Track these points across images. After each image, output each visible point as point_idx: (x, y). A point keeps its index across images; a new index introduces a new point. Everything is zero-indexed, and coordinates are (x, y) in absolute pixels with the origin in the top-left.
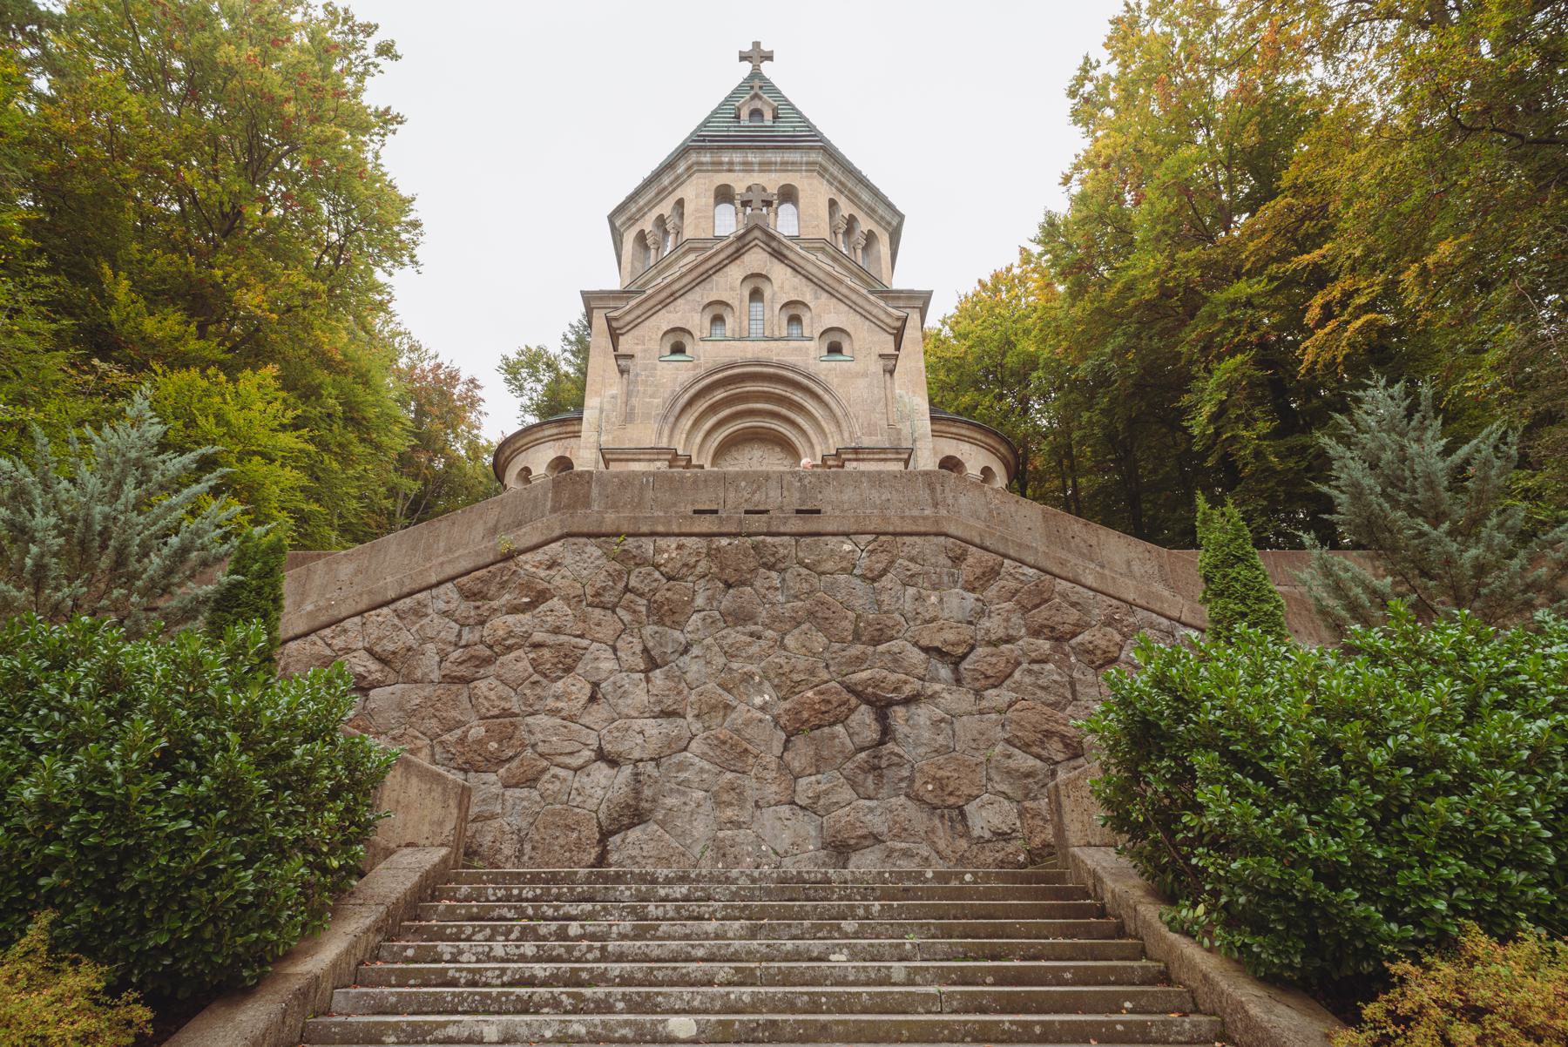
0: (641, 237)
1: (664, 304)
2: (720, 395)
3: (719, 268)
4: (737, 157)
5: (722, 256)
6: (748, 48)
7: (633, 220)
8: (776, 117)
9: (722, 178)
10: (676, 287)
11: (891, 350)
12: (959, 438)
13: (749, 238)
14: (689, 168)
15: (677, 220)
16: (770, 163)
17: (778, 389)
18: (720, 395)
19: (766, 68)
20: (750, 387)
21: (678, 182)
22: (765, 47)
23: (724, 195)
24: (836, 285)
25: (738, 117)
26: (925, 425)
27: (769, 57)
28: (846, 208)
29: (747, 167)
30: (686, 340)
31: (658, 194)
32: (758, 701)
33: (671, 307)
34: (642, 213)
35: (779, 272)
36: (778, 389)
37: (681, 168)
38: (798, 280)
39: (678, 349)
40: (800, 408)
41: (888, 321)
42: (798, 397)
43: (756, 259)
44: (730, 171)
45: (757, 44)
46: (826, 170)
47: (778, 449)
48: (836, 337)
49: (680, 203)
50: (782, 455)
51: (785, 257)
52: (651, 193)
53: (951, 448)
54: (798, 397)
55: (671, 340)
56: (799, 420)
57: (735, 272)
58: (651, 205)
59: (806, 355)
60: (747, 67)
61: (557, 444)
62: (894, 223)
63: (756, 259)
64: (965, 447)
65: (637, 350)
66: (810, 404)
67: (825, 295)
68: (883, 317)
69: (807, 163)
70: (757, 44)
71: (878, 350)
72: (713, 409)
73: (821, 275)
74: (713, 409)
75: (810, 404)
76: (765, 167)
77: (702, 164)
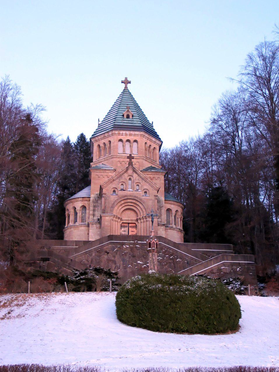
0: (99, 146)
1: (111, 182)
2: (123, 202)
3: (123, 174)
4: (124, 132)
5: (123, 172)
6: (124, 79)
7: (96, 141)
8: (133, 116)
9: (120, 137)
10: (114, 178)
11: (156, 194)
12: (171, 204)
13: (129, 167)
14: (112, 134)
15: (108, 145)
16: (131, 134)
17: (134, 201)
18: (123, 202)
19: (129, 85)
20: (129, 201)
21: (109, 136)
22: (129, 79)
23: (121, 140)
24: (146, 179)
25: (123, 116)
26: (164, 201)
27: (130, 83)
28: (149, 143)
29: (126, 135)
30: (116, 190)
31: (104, 137)
32: (136, 267)
33: (113, 183)
34: (99, 140)
35: (135, 175)
36: (134, 201)
37: (110, 133)
38: (138, 178)
39: (114, 191)
40: (138, 205)
41: (156, 188)
42: (138, 203)
43: (130, 171)
44: (122, 135)
45: (126, 78)
46: (144, 136)
47: (133, 212)
48: (146, 190)
49: (110, 141)
50: (134, 213)
51: (137, 172)
52: (102, 136)
53: (168, 206)
54: (138, 203)
55: (113, 190)
56: (138, 208)
57: (126, 175)
58: (102, 139)
59: (140, 193)
60: (123, 85)
61: (83, 202)
62: (160, 144)
63: (130, 171)
64: (172, 206)
65: (107, 192)
66: (140, 205)
67: (144, 181)
68: (155, 187)
69: (140, 135)
70: (126, 78)
71: (154, 194)
72: (121, 205)
73: (143, 177)
74: (121, 205)
75: (140, 205)
76: (130, 135)
77: (116, 133)
